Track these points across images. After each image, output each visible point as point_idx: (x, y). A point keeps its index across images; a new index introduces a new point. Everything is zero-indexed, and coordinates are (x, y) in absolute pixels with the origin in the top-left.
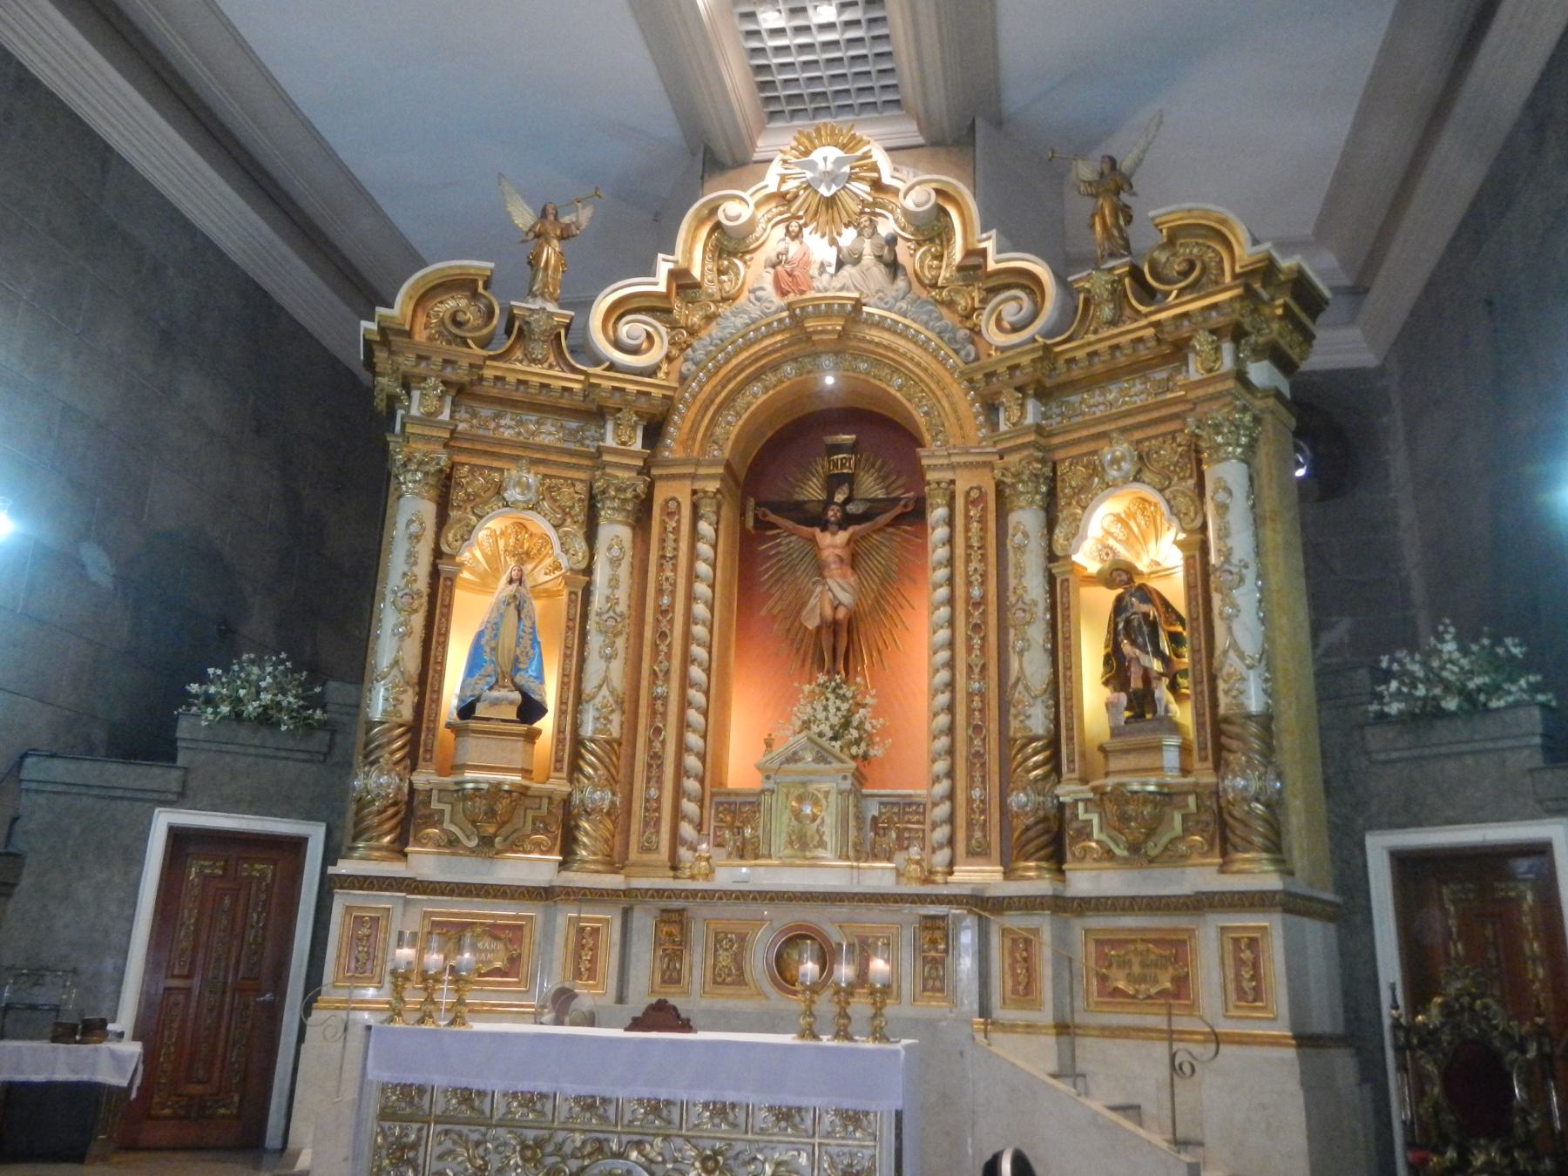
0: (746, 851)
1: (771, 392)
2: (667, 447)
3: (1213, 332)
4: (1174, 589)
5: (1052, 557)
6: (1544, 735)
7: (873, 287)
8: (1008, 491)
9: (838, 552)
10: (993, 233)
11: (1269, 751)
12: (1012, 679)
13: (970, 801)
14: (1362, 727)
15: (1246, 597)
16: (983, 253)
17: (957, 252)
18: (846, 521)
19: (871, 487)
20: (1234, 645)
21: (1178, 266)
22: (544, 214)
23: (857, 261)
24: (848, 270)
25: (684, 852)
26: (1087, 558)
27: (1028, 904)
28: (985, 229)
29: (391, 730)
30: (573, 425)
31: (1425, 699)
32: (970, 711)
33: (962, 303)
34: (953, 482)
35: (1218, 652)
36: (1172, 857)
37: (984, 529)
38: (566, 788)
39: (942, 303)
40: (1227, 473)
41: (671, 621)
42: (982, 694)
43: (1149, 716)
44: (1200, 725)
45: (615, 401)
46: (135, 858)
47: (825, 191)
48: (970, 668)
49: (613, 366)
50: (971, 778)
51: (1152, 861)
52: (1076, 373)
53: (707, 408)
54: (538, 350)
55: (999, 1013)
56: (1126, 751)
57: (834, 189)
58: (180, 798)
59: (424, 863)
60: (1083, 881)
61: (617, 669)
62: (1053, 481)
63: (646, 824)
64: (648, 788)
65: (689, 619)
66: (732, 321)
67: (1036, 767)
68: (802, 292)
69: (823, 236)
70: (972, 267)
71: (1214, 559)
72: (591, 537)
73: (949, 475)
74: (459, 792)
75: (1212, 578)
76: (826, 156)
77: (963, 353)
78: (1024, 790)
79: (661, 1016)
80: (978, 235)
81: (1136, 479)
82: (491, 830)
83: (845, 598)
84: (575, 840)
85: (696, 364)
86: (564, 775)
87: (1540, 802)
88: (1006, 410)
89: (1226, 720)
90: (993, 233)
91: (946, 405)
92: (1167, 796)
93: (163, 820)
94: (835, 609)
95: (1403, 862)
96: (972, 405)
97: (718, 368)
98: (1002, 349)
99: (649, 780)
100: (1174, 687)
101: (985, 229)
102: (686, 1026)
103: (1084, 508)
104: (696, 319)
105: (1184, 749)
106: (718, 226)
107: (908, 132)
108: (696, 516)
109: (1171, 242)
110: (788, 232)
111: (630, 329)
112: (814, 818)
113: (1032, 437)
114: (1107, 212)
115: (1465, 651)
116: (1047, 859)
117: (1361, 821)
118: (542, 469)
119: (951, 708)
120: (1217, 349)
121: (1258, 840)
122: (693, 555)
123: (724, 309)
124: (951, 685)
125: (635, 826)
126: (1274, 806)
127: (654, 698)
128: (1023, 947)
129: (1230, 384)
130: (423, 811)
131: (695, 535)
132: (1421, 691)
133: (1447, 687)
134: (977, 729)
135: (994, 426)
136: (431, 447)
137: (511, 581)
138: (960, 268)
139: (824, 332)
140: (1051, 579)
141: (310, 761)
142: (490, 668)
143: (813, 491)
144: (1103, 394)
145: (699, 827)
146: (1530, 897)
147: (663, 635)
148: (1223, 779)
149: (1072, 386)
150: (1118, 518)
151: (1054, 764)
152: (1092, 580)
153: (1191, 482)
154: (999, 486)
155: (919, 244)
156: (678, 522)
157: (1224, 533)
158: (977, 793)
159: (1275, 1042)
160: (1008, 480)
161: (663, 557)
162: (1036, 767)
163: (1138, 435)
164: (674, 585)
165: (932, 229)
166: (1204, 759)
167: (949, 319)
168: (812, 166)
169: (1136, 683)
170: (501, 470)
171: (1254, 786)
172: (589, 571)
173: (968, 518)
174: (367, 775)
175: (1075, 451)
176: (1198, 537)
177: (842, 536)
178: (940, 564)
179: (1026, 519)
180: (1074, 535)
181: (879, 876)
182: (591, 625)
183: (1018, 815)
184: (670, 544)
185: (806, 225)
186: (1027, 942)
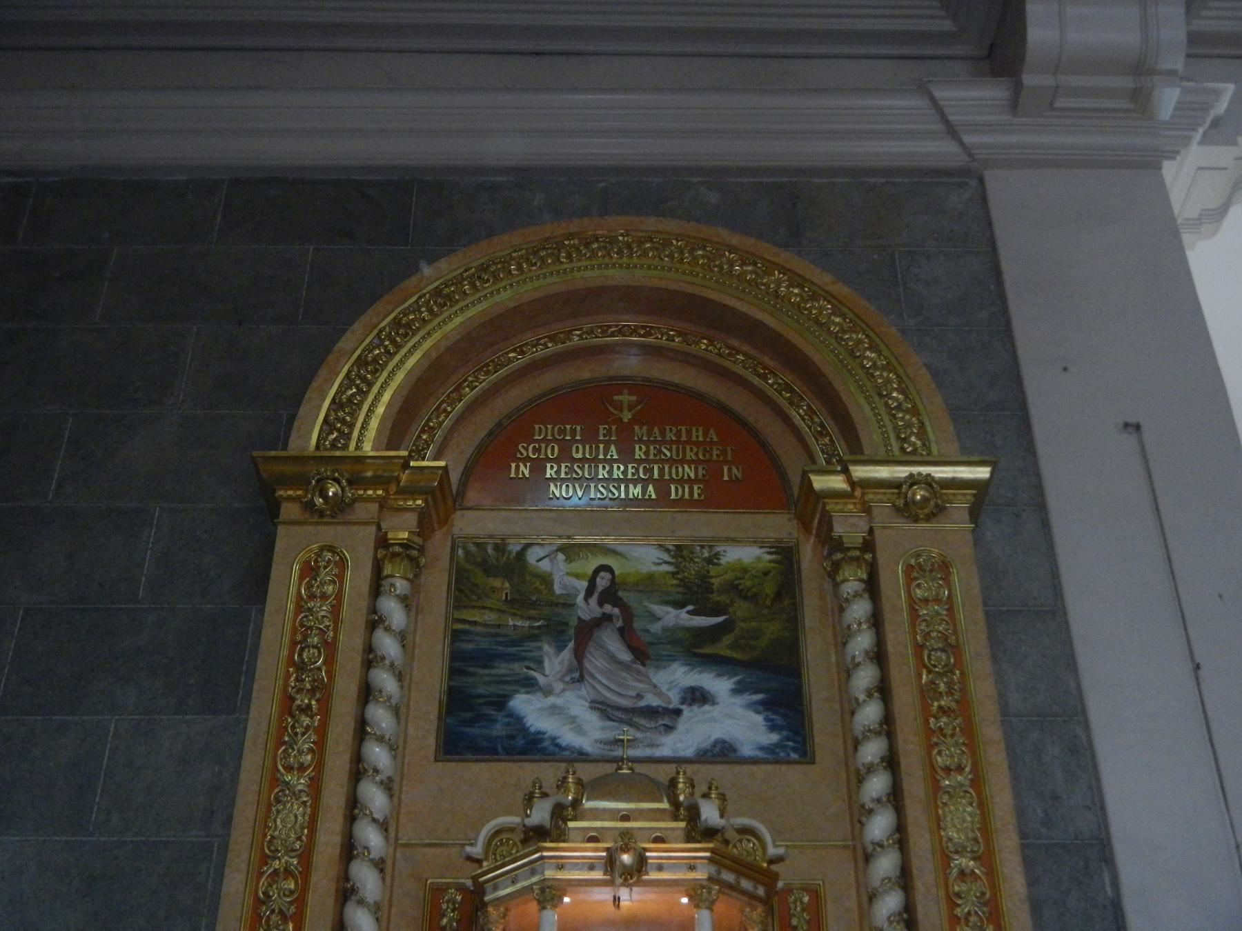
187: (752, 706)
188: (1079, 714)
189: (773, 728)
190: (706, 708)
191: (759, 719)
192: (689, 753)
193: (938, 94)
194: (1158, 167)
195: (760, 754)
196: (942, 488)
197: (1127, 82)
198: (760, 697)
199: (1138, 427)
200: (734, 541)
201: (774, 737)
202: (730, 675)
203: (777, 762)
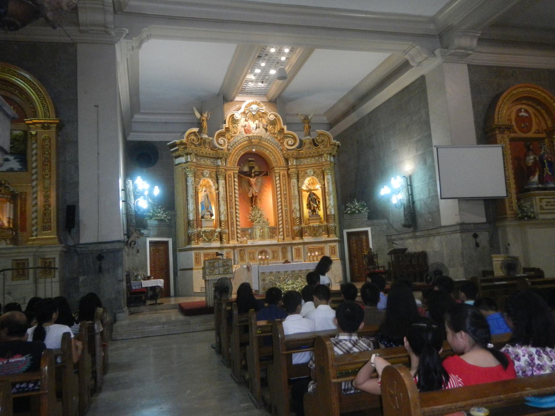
0: (252, 237)
1: (244, 153)
2: (227, 164)
3: (327, 154)
5: (298, 187)
6: (368, 216)
7: (263, 133)
8: (291, 176)
9: (255, 182)
10: (286, 126)
11: (334, 220)
12: (293, 208)
13: (286, 228)
14: (343, 214)
15: (332, 197)
16: (283, 129)
17: (278, 128)
18: (255, 176)
19: (256, 168)
20: (330, 204)
21: (320, 140)
22: (201, 115)
23: (259, 128)
24: (258, 129)
25: (239, 239)
26: (304, 188)
27: (299, 244)
28: (284, 125)
29: (194, 222)
30: (212, 160)
31: (353, 211)
32: (285, 213)
33: (279, 138)
34: (280, 172)
35: (327, 205)
36: (320, 235)
37: (286, 181)
38: (220, 229)
40: (329, 177)
41: (232, 198)
42: (287, 210)
43: (314, 214)
44: (324, 216)
45: (221, 156)
47: (253, 113)
48: (285, 206)
49: (219, 149)
50: (286, 224)
51: (317, 236)
52: (303, 156)
53: (233, 155)
54: (207, 146)
55: (294, 260)
56: (312, 220)
57: (255, 113)
59: (201, 245)
60: (306, 239)
61: (226, 206)
62: (298, 174)
63: (232, 234)
64: (231, 228)
65: (235, 197)
66: (237, 139)
67: (298, 222)
68: (250, 133)
69: (252, 121)
70: (282, 130)
71: (327, 190)
72: (218, 183)
73: (279, 171)
74: (204, 232)
75: (326, 193)
76: (254, 107)
77: (280, 148)
78: (297, 226)
79: (287, 262)
80: (282, 126)
81: (313, 176)
82: (210, 238)
83: (257, 191)
84: (223, 238)
85: (231, 147)
86: (219, 227)
87: (367, 225)
88: (290, 161)
89: (329, 215)
90: (286, 126)
91: (277, 157)
92: (319, 227)
94: (256, 193)
95: (349, 234)
96: (282, 158)
97: (235, 147)
99: (231, 227)
100: (319, 209)
101: (284, 125)
102: (290, 263)
103: (304, 179)
104: (229, 137)
106: (233, 118)
107: (265, 99)
108: (234, 178)
109: (319, 136)
110: (246, 120)
111: (221, 141)
112: (263, 232)
113: (295, 167)
114: (307, 126)
115: (358, 203)
116: (300, 236)
117: (342, 228)
118: (209, 169)
120: (327, 157)
121: (334, 232)
122: (235, 185)
123: (235, 135)
124: (282, 209)
125: (230, 235)
126: (335, 227)
127: (231, 212)
128: (298, 250)
129: (330, 163)
130: (199, 235)
131: (234, 181)
132: (353, 210)
133: (356, 209)
134: (287, 216)
136: (193, 167)
137: (205, 191)
138: (278, 131)
139: (255, 142)
140: (299, 191)
141: (167, 227)
142: (205, 209)
143: (246, 169)
144: (307, 160)
145: (239, 234)
146: (364, 238)
147: (231, 200)
148: (329, 224)
149: (302, 158)
150: (308, 181)
151: (300, 221)
152: (305, 191)
153: (322, 177)
154: (289, 175)
155: (270, 125)
156: (231, 179)
158: (287, 226)
159: (337, 260)
160: (291, 174)
161: (229, 186)
162: (298, 222)
163: (313, 168)
164: (232, 191)
165: (273, 123)
166: (325, 221)
167: (277, 141)
168: (252, 108)
169: (312, 208)
170: (203, 170)
171: (333, 225)
172: (218, 189)
173: (283, 179)
174: (192, 230)
175: (302, 169)
176: (324, 187)
177: (255, 179)
178: (279, 187)
179: (294, 181)
180: (302, 184)
181: (274, 242)
182: (221, 199)
183: (296, 230)
184: (230, 184)
185: (248, 118)
186: (299, 250)
187: (18, 162)
188: (78, 161)
189: (21, 165)
190: (8, 162)
191: (18, 164)
192: (5, 170)
193: (65, 28)
194: (114, 44)
195: (18, 170)
196: (50, 124)
197: (103, 29)
198: (19, 160)
199: (98, 106)
200: (15, 130)
201: (21, 167)
202: (13, 156)
203: (21, 171)
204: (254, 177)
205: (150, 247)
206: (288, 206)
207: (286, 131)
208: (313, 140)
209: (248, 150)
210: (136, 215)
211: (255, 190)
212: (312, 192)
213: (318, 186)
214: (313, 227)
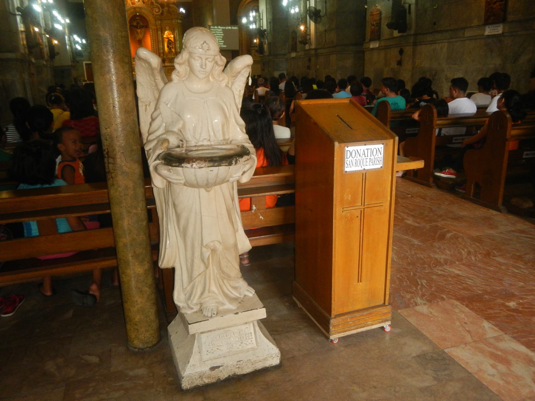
3: (176, 19)
4: (172, 39)
20: (177, 46)
24: (139, 2)
26: (165, 36)
33: (151, 7)
39: (149, 7)
40: (176, 32)
46: (83, 66)
58: (85, 61)
71: (176, 39)
93: (84, 63)
98: (157, 15)
100: (173, 48)
105: (174, 54)
119: (154, 49)
124: (154, 47)
135: (156, 23)
143: (135, 24)
154: (157, 29)
157: (176, 37)
169: (170, 48)
179: (159, 32)
204: (140, 29)
205: (86, 66)
206: (157, 46)
207: (155, 4)
208: (169, 10)
209: (134, 14)
210: (76, 53)
211: (140, 36)
212: (170, 38)
213: (172, 36)
214: (169, 58)
